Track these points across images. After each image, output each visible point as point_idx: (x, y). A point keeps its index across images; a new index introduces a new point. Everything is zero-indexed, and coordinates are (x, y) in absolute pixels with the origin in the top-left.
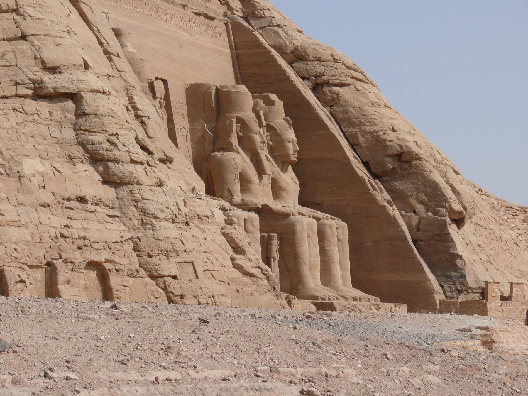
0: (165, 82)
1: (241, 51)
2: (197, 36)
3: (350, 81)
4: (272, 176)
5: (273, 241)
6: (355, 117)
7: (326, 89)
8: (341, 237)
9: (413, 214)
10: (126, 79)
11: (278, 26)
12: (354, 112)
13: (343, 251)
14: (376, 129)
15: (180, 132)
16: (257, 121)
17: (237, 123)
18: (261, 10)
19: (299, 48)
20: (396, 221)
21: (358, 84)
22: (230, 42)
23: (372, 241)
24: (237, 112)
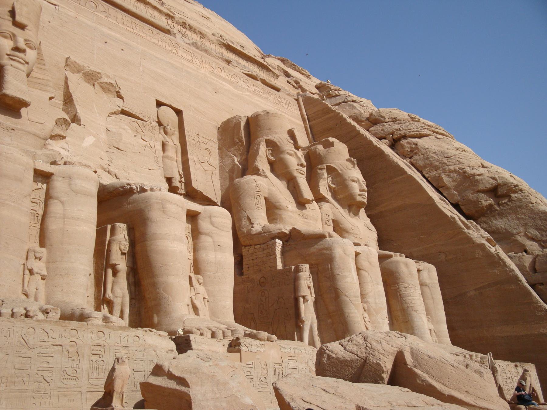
0: (179, 112)
1: (314, 122)
2: (248, 93)
4: (332, 217)
7: (404, 142)
8: (428, 281)
9: (524, 254)
11: (353, 101)
12: (435, 157)
13: (433, 299)
14: (461, 166)
15: (199, 166)
17: (267, 147)
18: (336, 90)
19: (374, 113)
20: (500, 258)
21: (440, 136)
22: (302, 116)
23: (475, 290)
24: (267, 135)
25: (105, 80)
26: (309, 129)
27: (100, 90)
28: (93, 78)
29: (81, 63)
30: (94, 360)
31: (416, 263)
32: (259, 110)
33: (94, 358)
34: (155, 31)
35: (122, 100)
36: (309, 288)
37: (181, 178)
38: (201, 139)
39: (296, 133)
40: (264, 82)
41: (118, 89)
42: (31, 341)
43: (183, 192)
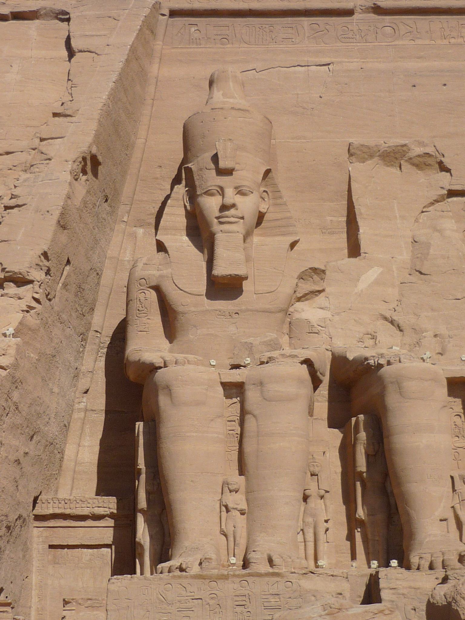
10: (44, 150)
25: (418, 150)
28: (397, 156)
29: (371, 141)
30: (239, 612)
33: (239, 609)
35: (449, 174)
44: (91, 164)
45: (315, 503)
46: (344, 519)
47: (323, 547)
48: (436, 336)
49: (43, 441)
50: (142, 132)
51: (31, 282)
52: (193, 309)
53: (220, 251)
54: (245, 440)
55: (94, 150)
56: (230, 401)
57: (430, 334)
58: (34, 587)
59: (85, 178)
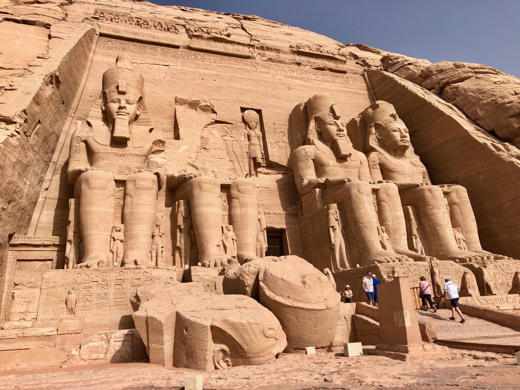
0: (259, 112)
3: (470, 74)
5: (330, 211)
6: (474, 98)
7: (447, 88)
8: (457, 200)
11: (410, 64)
12: (473, 95)
13: (462, 213)
14: (494, 98)
15: (275, 145)
16: (332, 114)
18: (395, 59)
21: (482, 75)
22: (367, 87)
23: (510, 201)
24: (316, 114)
26: (374, 96)
27: (202, 111)
29: (185, 98)
31: (441, 187)
32: (311, 96)
33: (117, 287)
34: (239, 59)
36: (337, 220)
37: (263, 156)
38: (277, 126)
39: (334, 107)
40: (331, 70)
41: (212, 108)
42: (79, 281)
43: (265, 165)
44: (54, 80)
45: (157, 238)
46: (170, 247)
47: (160, 259)
48: (212, 172)
49: (18, 206)
50: (83, 80)
51: (15, 123)
52: (103, 151)
53: (117, 126)
54: (125, 207)
55: (57, 74)
56: (118, 189)
57: (210, 170)
58: (6, 281)
59: (51, 86)
